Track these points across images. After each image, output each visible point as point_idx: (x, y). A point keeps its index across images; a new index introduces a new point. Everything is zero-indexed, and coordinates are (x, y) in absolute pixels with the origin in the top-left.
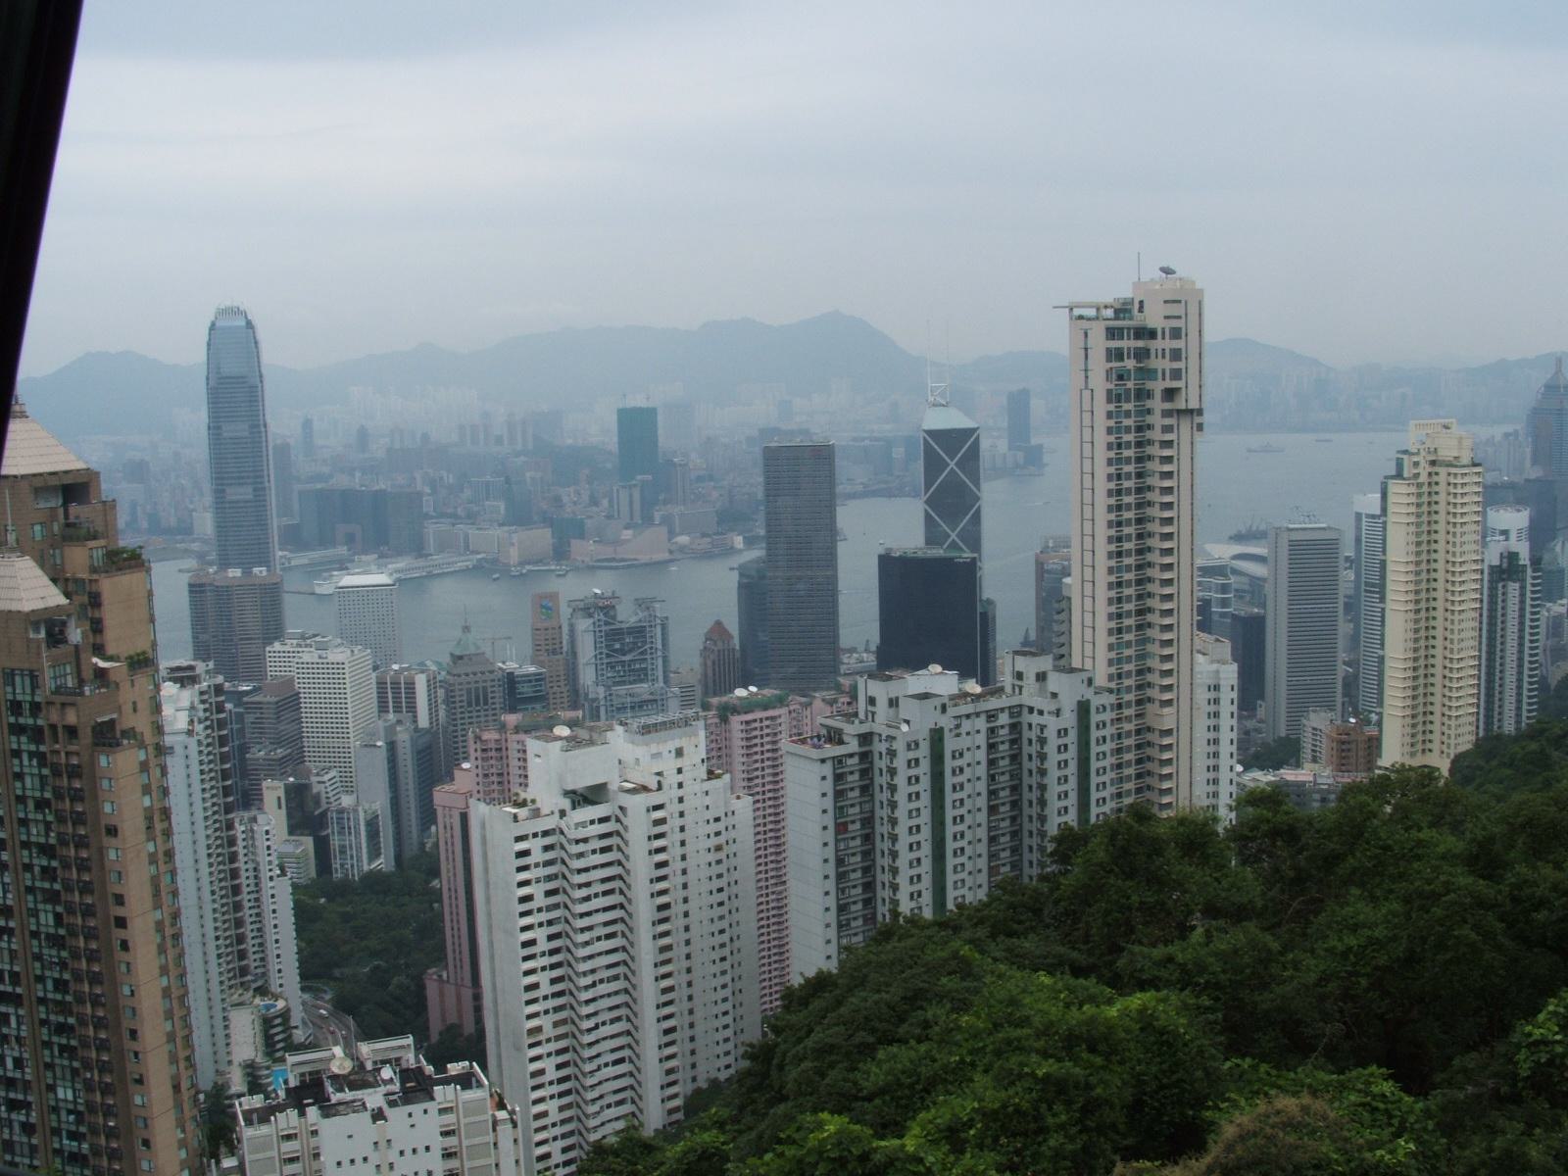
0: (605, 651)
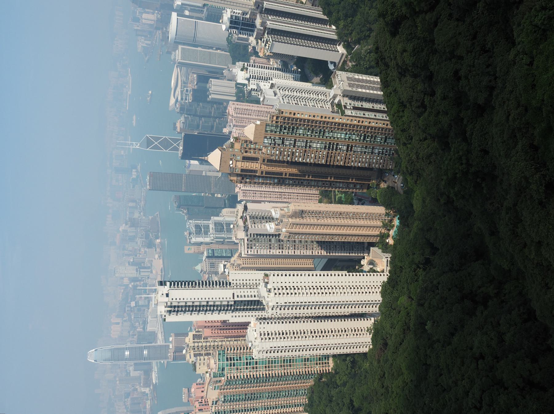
0: (201, 235)
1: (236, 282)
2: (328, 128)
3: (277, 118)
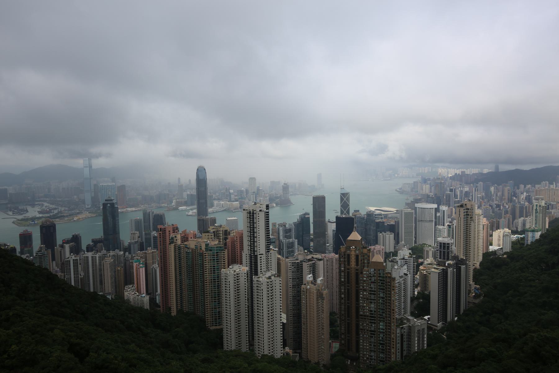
2: (386, 315)
3: (390, 277)
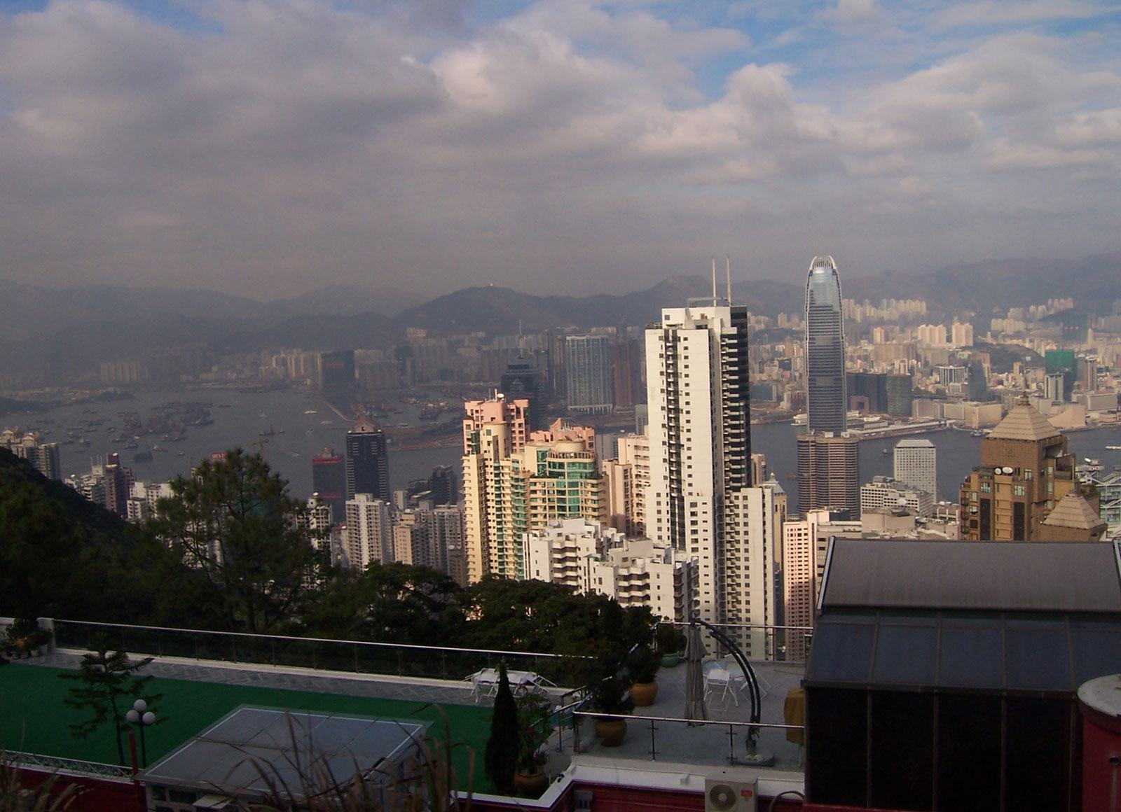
1: (741, 507)
